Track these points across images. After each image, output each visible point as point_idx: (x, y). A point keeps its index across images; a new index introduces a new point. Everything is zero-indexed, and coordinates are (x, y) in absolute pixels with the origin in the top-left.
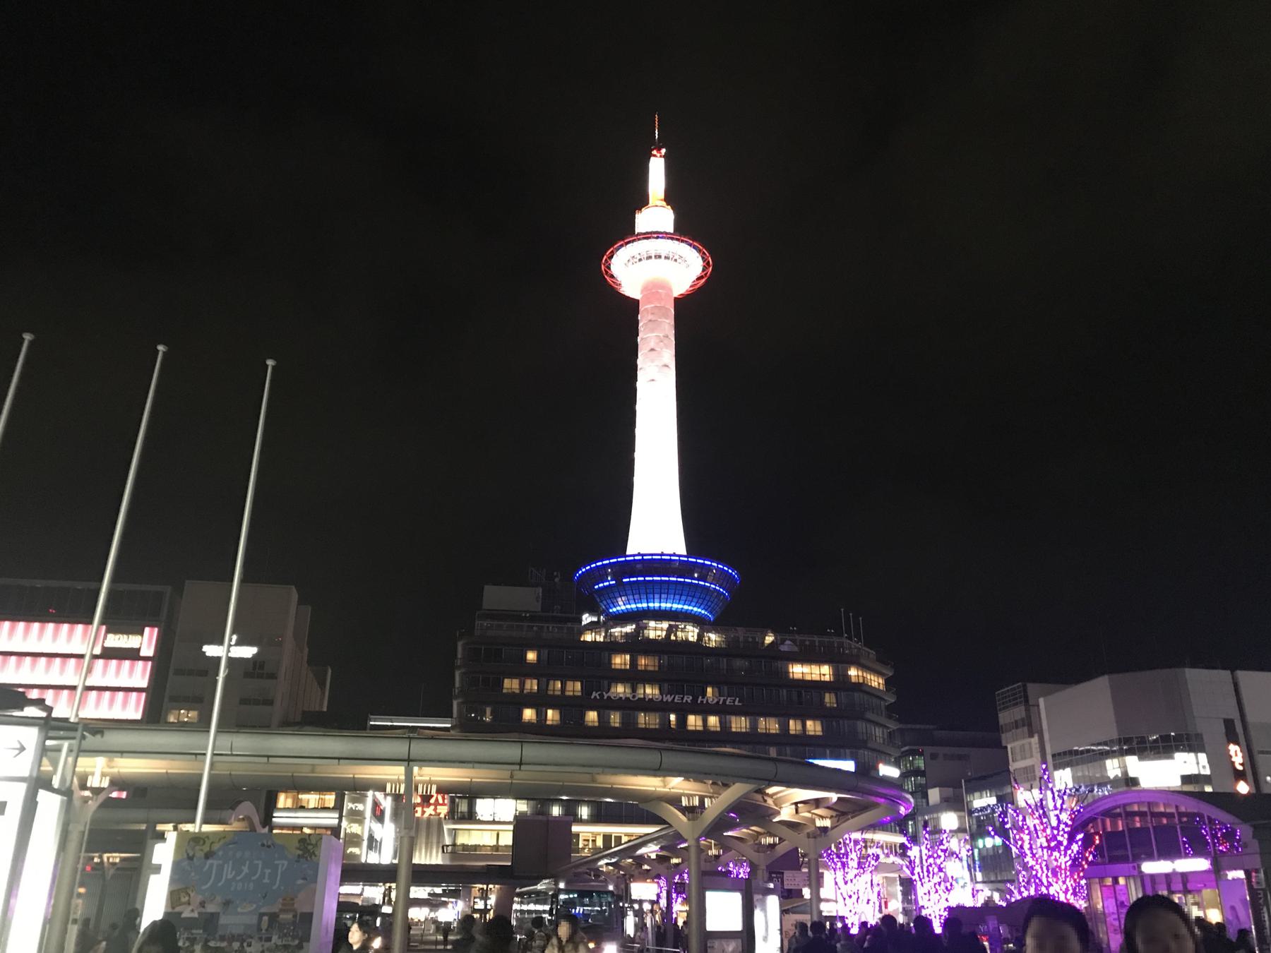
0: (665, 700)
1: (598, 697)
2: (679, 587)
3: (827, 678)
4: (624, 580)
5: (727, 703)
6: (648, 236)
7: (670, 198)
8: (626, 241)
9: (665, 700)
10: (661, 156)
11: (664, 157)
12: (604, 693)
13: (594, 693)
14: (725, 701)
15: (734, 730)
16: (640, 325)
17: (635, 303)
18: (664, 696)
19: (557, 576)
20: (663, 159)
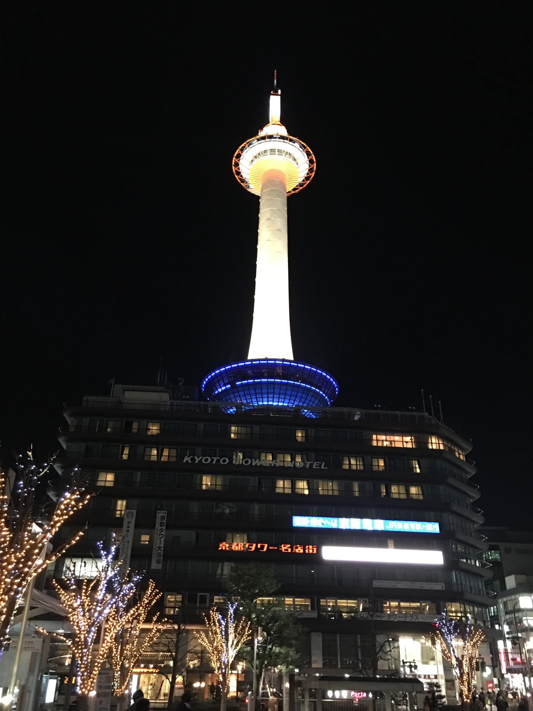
0: (254, 464)
1: (190, 461)
2: (284, 387)
3: (409, 446)
4: (237, 383)
5: (314, 467)
6: (263, 138)
7: (283, 121)
8: (247, 141)
9: (254, 464)
10: (277, 95)
11: (280, 95)
12: (196, 458)
13: (186, 457)
14: (311, 465)
15: (321, 493)
16: (261, 204)
17: (258, 198)
18: (253, 460)
19: (181, 381)
20: (279, 97)
